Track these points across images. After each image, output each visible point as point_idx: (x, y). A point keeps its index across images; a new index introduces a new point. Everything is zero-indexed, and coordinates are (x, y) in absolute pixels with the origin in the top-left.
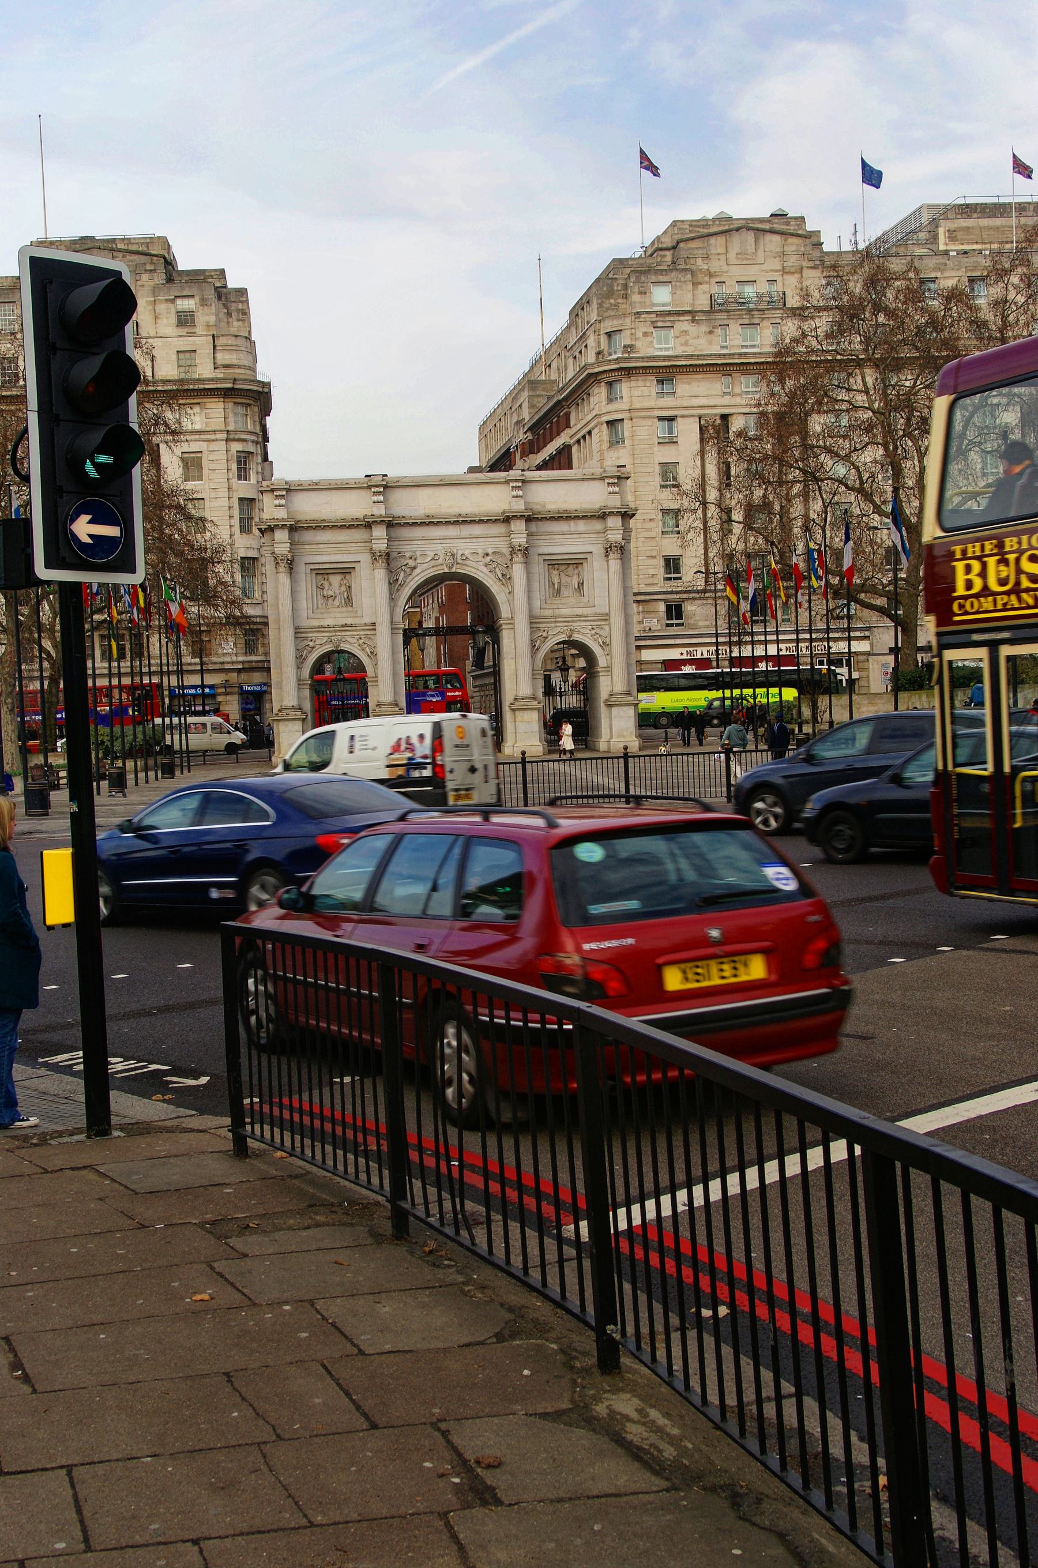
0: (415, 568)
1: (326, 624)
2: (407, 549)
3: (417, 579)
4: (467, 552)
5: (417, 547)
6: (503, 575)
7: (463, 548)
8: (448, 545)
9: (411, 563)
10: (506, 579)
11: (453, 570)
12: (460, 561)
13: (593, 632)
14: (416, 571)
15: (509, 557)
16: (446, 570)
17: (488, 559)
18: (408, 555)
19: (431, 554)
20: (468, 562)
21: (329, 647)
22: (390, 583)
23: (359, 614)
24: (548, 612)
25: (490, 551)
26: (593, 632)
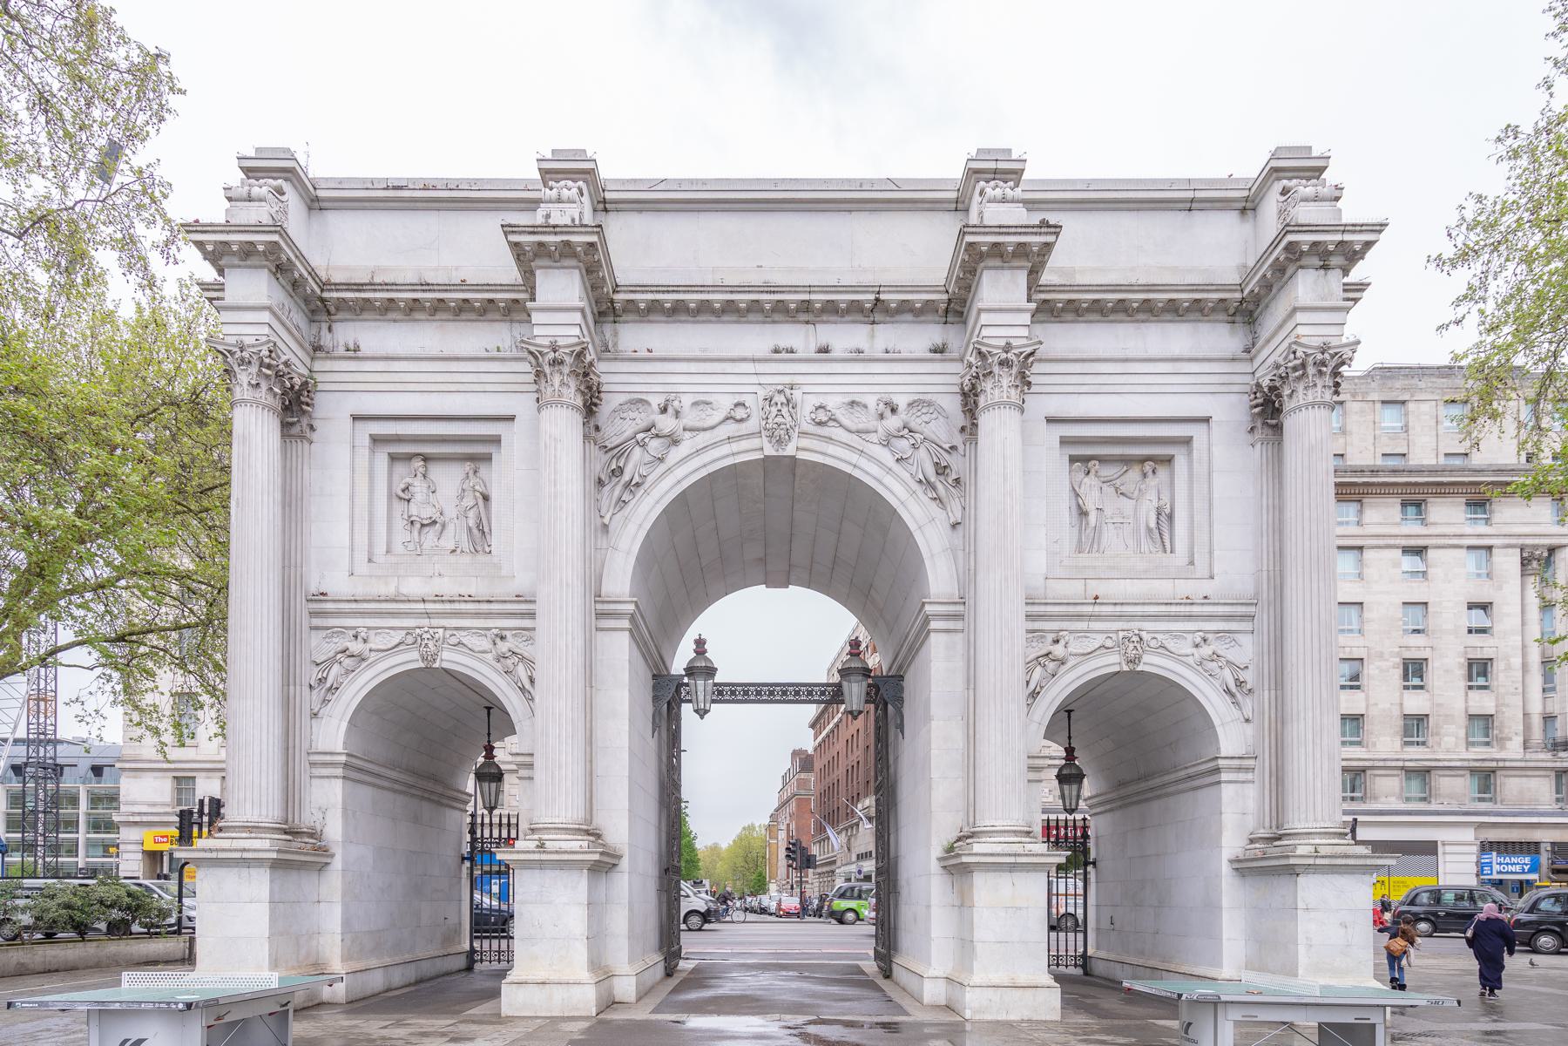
0: (674, 441)
1: (404, 590)
2: (651, 384)
3: (680, 472)
4: (833, 403)
5: (686, 383)
6: (941, 470)
7: (822, 387)
8: (779, 374)
9: (666, 423)
10: (947, 478)
11: (790, 450)
12: (812, 429)
13: (1206, 651)
14: (684, 449)
15: (960, 420)
16: (770, 450)
17: (893, 423)
18: (656, 401)
19: (725, 404)
20: (834, 432)
21: (410, 660)
22: (600, 483)
23: (504, 572)
24: (1073, 589)
25: (901, 401)
26: (1206, 651)
